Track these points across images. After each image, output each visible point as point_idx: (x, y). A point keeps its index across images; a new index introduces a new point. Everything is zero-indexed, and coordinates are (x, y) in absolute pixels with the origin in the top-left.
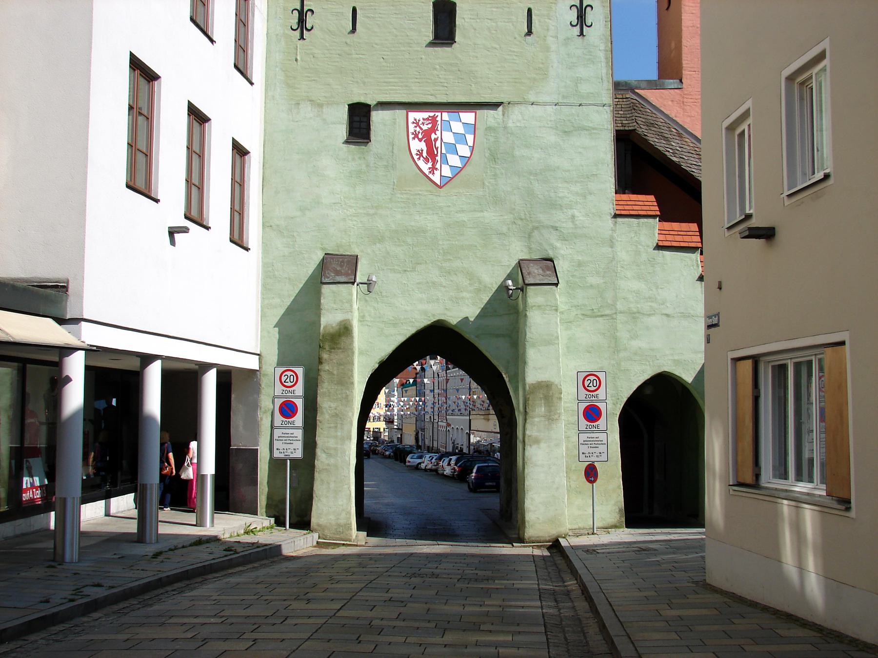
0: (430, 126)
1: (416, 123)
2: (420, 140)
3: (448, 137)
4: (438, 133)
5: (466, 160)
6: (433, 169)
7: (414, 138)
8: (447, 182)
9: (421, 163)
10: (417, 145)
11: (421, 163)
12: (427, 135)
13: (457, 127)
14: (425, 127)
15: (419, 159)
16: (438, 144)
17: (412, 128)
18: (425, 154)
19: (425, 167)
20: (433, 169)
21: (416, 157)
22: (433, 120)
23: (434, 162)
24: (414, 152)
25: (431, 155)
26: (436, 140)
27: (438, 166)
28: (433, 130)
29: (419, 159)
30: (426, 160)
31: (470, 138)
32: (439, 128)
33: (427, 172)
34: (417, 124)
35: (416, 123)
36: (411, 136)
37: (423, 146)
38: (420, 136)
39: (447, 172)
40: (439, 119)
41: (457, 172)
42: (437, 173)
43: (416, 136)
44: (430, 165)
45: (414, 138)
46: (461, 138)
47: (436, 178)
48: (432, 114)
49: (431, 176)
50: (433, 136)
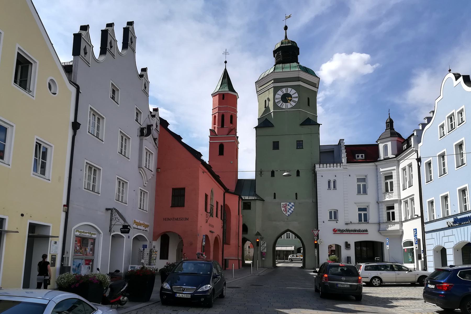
3: (289, 207)
13: (291, 205)
20: (286, 213)
22: (286, 204)
25: (286, 211)
31: (293, 207)
46: (291, 207)
47: (287, 215)
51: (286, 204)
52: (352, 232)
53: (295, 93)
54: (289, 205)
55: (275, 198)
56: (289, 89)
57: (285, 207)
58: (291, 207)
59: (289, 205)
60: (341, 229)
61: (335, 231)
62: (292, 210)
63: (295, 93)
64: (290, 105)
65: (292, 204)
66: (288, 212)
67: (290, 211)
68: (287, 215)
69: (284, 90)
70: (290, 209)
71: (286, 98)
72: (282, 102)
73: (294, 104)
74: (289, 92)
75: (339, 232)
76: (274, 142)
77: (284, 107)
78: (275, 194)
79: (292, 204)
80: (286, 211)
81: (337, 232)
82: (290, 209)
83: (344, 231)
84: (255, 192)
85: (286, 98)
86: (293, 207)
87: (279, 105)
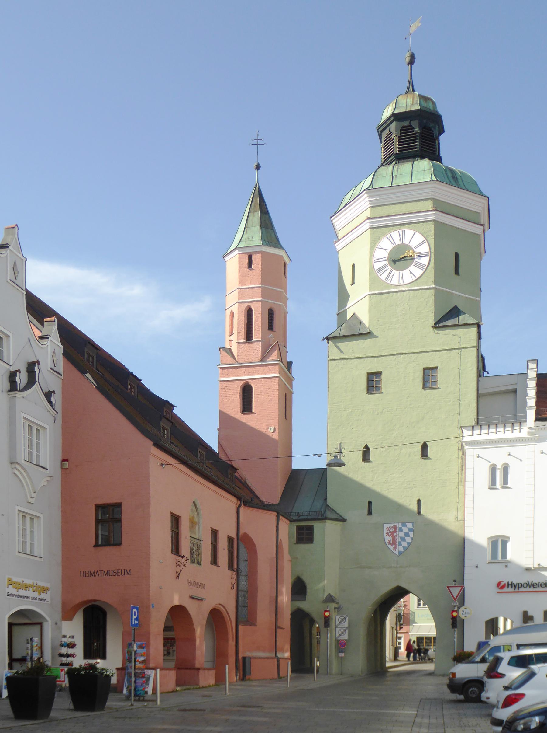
1: (388, 529)
3: (402, 534)
5: (409, 544)
6: (395, 549)
8: (401, 553)
9: (390, 546)
10: (388, 538)
11: (390, 546)
13: (405, 530)
14: (392, 531)
16: (397, 537)
17: (386, 531)
18: (391, 542)
19: (391, 548)
20: (395, 549)
21: (387, 544)
22: (395, 527)
23: (396, 545)
24: (387, 541)
25: (394, 543)
26: (396, 535)
27: (397, 547)
28: (395, 531)
30: (392, 545)
31: (411, 534)
33: (392, 550)
34: (388, 530)
35: (388, 529)
36: (385, 535)
37: (390, 538)
39: (401, 549)
41: (406, 549)
43: (388, 534)
44: (394, 546)
46: (407, 534)
49: (394, 551)
50: (395, 534)
51: (395, 527)
52: (540, 589)
53: (423, 243)
54: (401, 530)
55: (370, 513)
56: (409, 233)
57: (392, 534)
58: (407, 534)
59: (401, 530)
60: (515, 582)
61: (501, 586)
63: (423, 243)
64: (409, 275)
65: (410, 525)
66: (400, 544)
67: (404, 544)
68: (397, 552)
69: (395, 235)
70: (403, 539)
71: (400, 258)
72: (389, 268)
73: (418, 272)
74: (406, 242)
75: (510, 589)
76: (370, 374)
77: (395, 281)
78: (370, 503)
79: (410, 525)
80: (394, 543)
81: (506, 589)
82: (403, 539)
83: (522, 585)
84: (326, 499)
85: (400, 258)
86: (411, 534)
87: (383, 277)
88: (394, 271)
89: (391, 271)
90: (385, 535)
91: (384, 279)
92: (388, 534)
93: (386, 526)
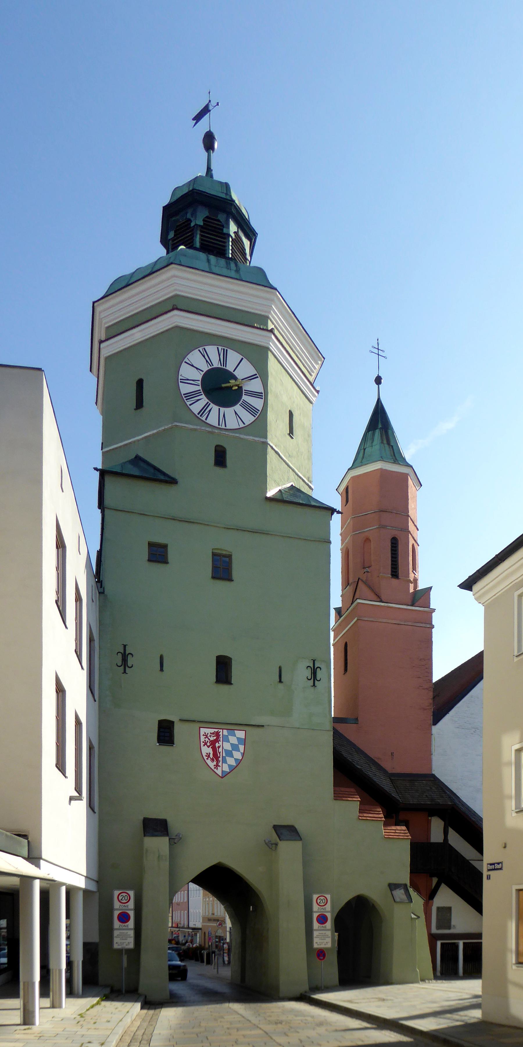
0: (215, 738)
2: (208, 747)
3: (227, 746)
4: (221, 743)
5: (239, 762)
6: (217, 766)
7: (204, 745)
9: (209, 762)
10: (206, 750)
12: (213, 743)
13: (233, 740)
14: (212, 739)
15: (207, 759)
16: (220, 750)
18: (211, 756)
19: (212, 764)
20: (217, 766)
21: (205, 758)
22: (217, 734)
23: (218, 761)
24: (204, 754)
25: (216, 757)
26: (219, 747)
27: (220, 764)
28: (217, 740)
29: (207, 759)
30: (212, 760)
32: (221, 740)
36: (202, 744)
37: (210, 750)
38: (208, 744)
40: (221, 733)
41: (232, 769)
42: (220, 769)
44: (215, 763)
45: (204, 745)
46: (235, 747)
47: (219, 772)
48: (216, 730)
49: (215, 770)
50: (217, 745)
58: (235, 747)
62: (238, 755)
66: (224, 761)
70: (229, 754)
82: (229, 754)
88: (212, 405)
89: (207, 405)
90: (202, 744)
91: (196, 413)
92: (206, 744)
93: (203, 731)
